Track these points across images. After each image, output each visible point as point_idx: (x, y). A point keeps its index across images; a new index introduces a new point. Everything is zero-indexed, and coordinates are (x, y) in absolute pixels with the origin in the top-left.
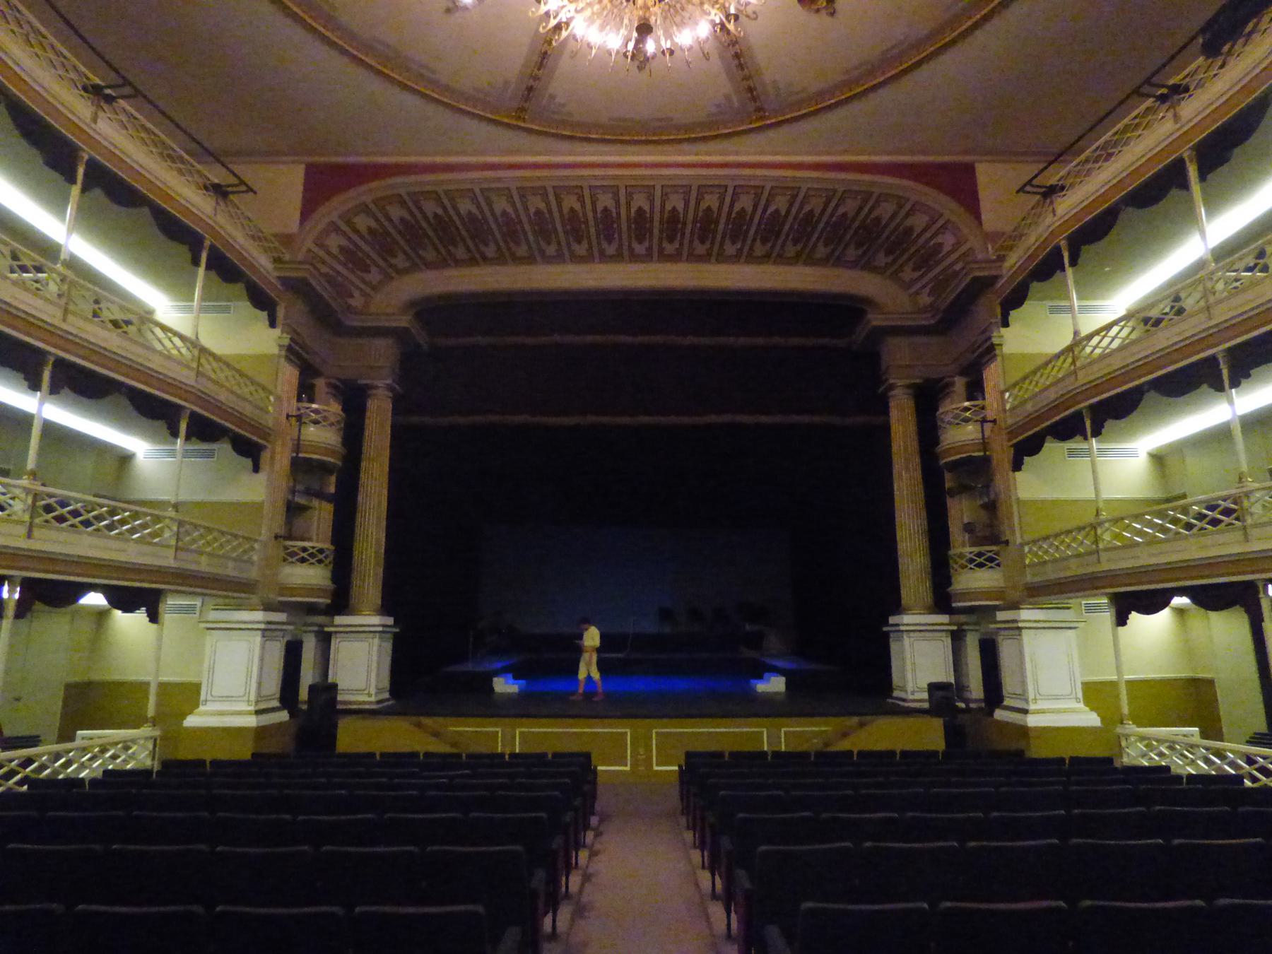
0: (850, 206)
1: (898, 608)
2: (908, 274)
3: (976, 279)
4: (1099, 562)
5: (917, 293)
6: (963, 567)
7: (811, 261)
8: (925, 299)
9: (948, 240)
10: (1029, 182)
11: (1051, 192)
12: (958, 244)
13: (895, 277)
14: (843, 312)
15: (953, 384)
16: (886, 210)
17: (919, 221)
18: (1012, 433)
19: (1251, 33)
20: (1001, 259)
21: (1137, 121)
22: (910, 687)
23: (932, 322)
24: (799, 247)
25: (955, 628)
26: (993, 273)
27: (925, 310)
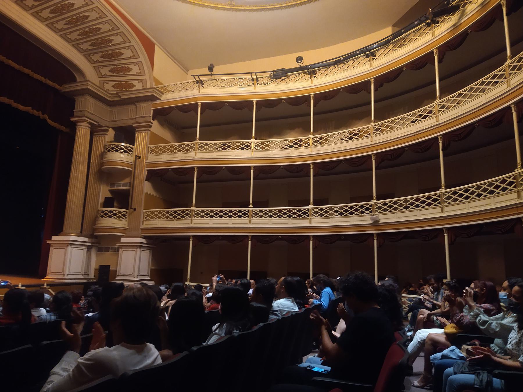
0: (105, 27)
1: (59, 230)
2: (105, 71)
3: (153, 95)
4: (191, 223)
5: (105, 82)
6: (102, 216)
7: (65, 37)
8: (109, 87)
9: (135, 69)
10: (198, 76)
11: (200, 83)
12: (140, 74)
13: (97, 69)
14: (65, 71)
15: (107, 131)
16: (118, 39)
17: (127, 53)
18: (148, 165)
19: (283, 80)
20: (163, 94)
21: (241, 80)
22: (67, 272)
23: (111, 100)
24: (65, 27)
25: (90, 244)
26: (159, 97)
27: (109, 92)
